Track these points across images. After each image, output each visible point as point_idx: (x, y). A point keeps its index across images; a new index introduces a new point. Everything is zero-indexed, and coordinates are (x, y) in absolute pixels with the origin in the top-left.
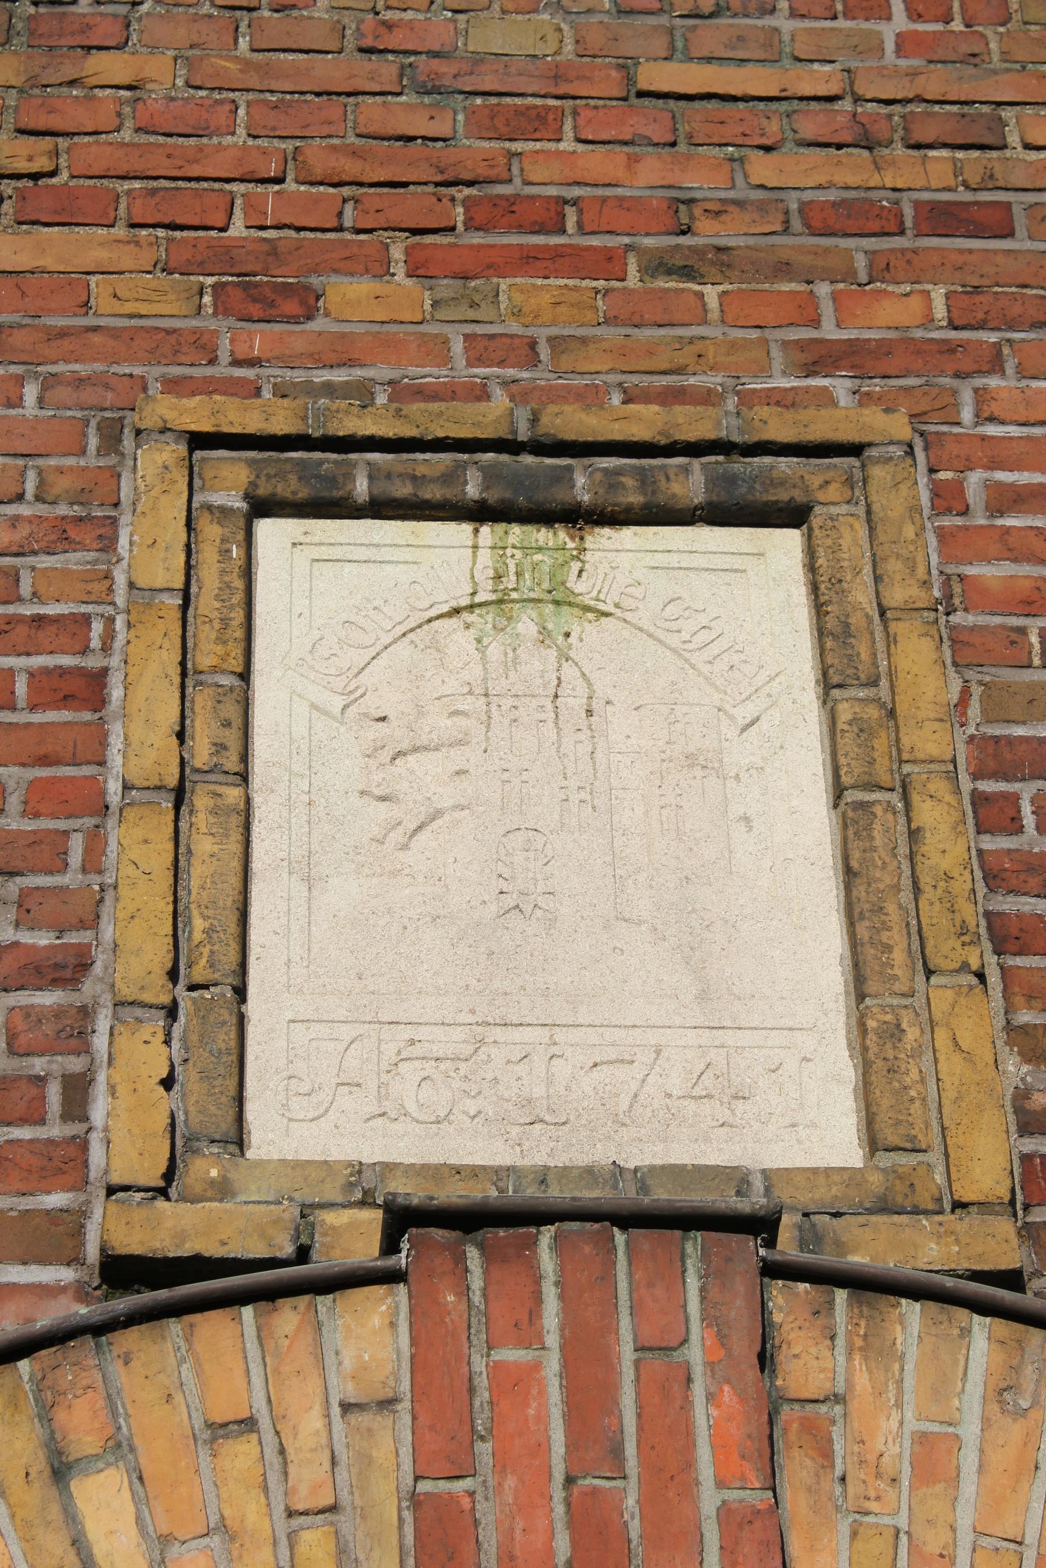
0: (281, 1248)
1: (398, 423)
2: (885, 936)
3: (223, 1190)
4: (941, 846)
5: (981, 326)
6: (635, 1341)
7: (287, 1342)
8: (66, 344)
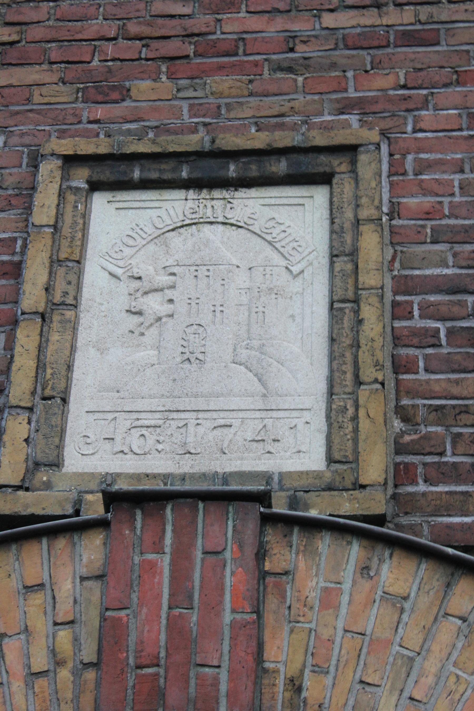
0: (68, 511)
1: (153, 146)
2: (344, 368)
3: (48, 486)
4: (371, 326)
5: (420, 88)
6: (203, 549)
7: (60, 551)
8: (19, 118)
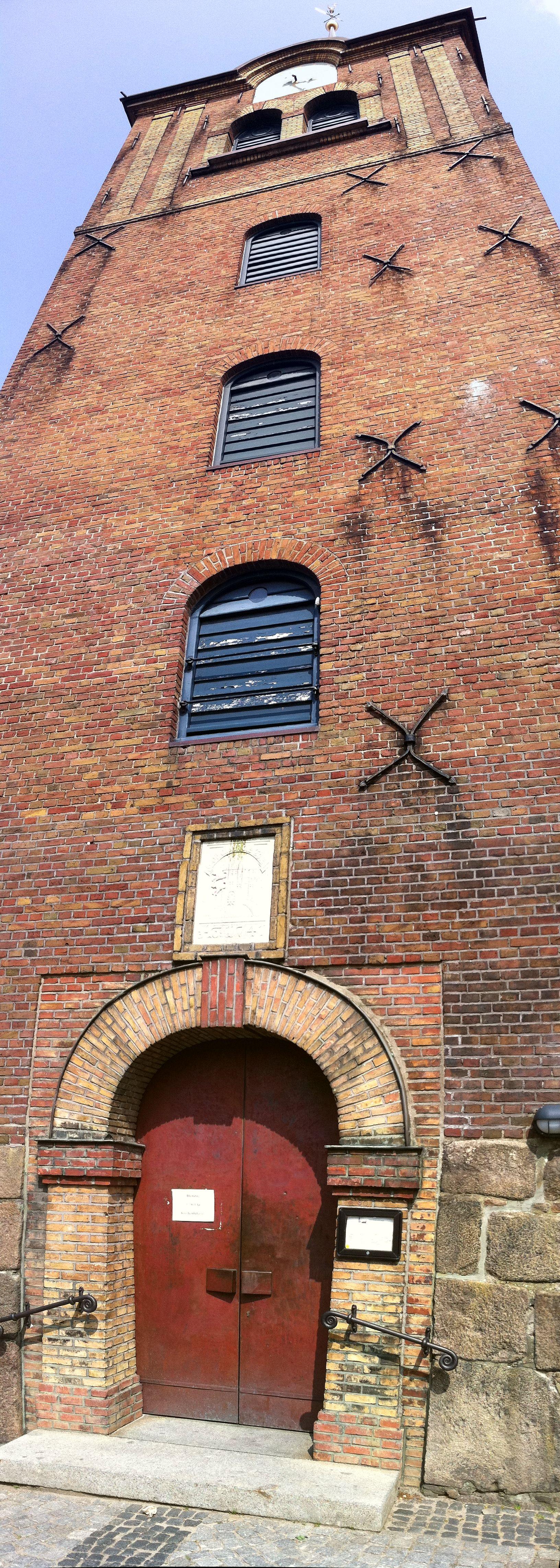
3: (188, 950)
